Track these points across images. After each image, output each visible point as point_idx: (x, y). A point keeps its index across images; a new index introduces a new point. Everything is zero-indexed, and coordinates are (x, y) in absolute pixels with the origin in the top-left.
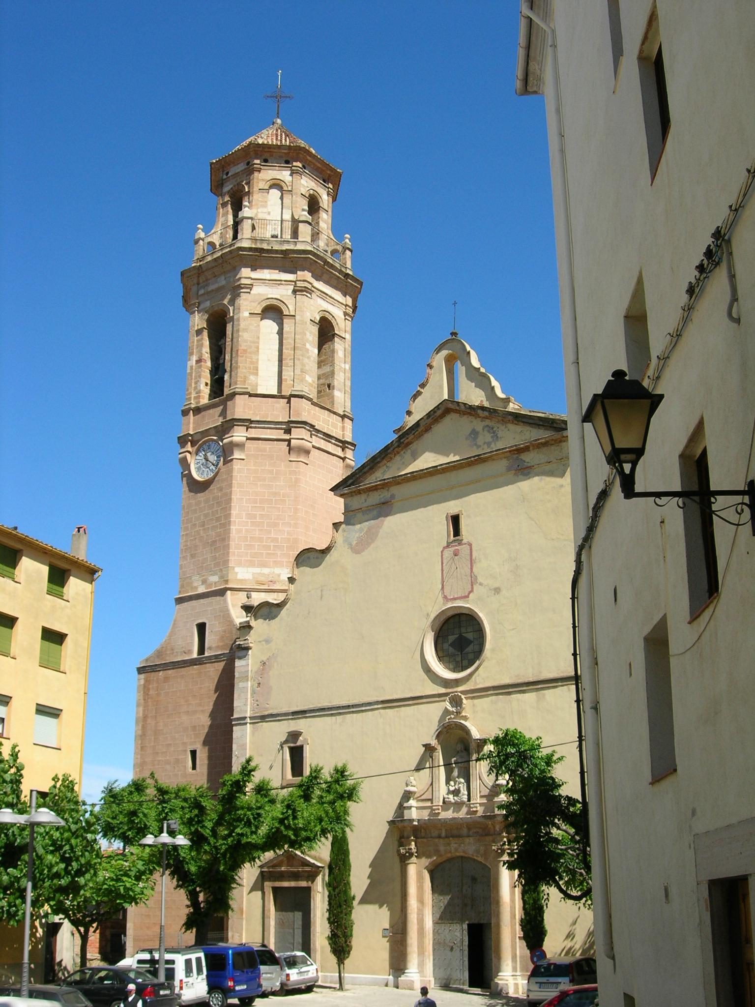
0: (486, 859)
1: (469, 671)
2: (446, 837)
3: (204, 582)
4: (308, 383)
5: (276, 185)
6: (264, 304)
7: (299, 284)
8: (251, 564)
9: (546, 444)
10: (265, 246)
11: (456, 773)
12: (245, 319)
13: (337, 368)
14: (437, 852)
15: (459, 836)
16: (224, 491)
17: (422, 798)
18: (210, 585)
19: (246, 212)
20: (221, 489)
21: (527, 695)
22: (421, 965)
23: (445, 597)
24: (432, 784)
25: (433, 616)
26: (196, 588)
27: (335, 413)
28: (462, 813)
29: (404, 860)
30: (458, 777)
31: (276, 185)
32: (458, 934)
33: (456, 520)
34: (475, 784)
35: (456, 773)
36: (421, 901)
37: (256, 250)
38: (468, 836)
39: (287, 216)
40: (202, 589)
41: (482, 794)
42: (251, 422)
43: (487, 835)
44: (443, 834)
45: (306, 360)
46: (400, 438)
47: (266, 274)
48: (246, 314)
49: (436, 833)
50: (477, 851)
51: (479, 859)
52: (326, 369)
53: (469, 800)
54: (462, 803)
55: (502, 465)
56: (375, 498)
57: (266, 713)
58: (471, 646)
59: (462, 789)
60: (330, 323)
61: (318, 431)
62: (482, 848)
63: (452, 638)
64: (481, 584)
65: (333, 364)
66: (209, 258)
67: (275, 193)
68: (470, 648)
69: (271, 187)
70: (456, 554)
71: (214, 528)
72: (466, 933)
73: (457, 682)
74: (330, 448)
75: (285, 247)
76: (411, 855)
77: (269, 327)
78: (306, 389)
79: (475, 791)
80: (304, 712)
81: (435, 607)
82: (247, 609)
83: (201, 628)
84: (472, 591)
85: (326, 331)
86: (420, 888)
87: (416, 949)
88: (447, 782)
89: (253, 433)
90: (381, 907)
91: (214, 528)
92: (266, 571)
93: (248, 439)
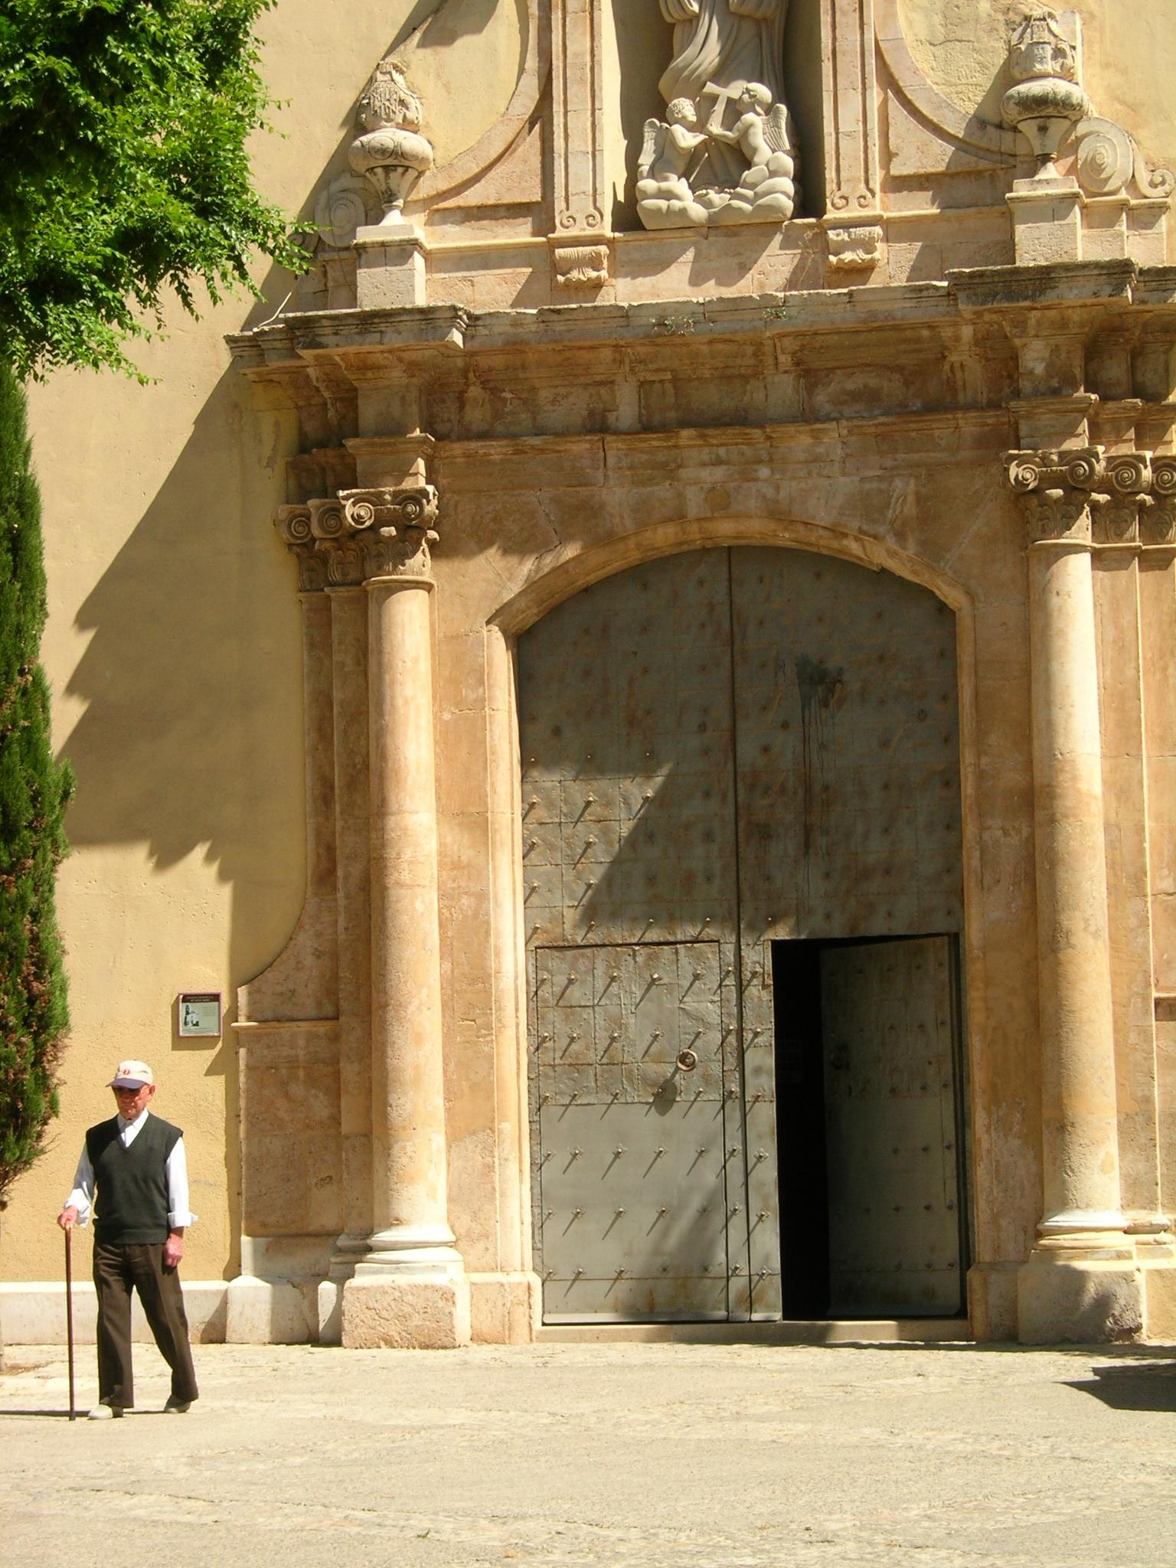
0: (932, 551)
2: (646, 427)
11: (705, 50)
14: (580, 516)
15: (741, 419)
17: (472, 197)
22: (471, 1198)
24: (541, 115)
28: (772, 271)
29: (341, 578)
30: (722, 74)
32: (708, 1006)
34: (847, 113)
35: (705, 50)
36: (468, 814)
38: (807, 416)
41: (897, 170)
43: (933, 407)
44: (626, 409)
49: (576, 404)
50: (871, 507)
51: (884, 554)
53: (810, 196)
54: (764, 226)
59: (759, 139)
62: (904, 488)
72: (761, 998)
76: (411, 532)
79: (851, 148)
86: (461, 738)
87: (438, 1102)
88: (645, 103)
90: (167, 856)
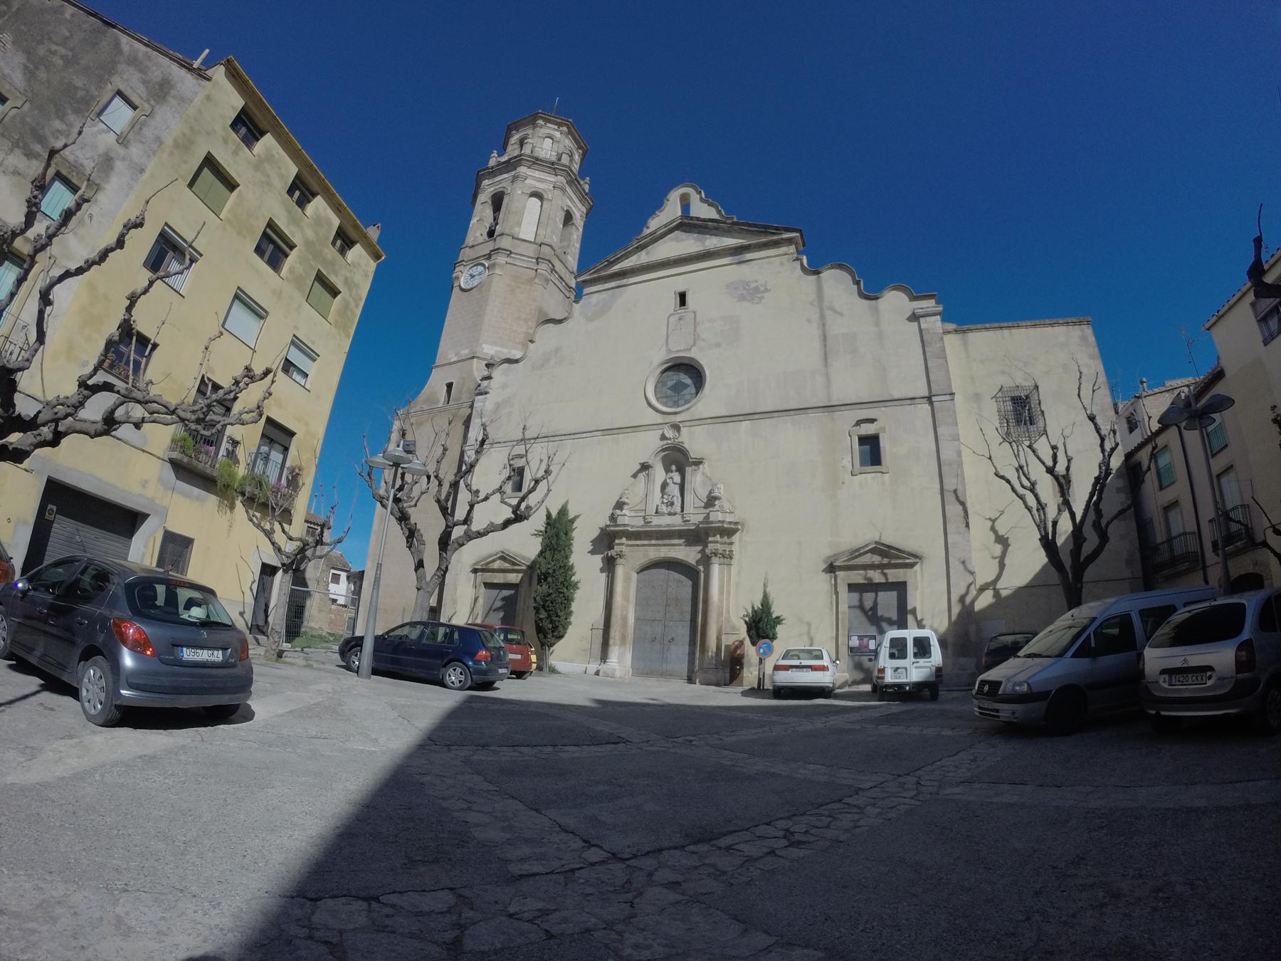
8: (494, 344)
23: (669, 351)
33: (682, 298)
47: (537, 174)
52: (565, 244)
63: (670, 383)
73: (675, 413)
81: (659, 357)
83: (450, 386)
85: (568, 218)
92: (505, 350)
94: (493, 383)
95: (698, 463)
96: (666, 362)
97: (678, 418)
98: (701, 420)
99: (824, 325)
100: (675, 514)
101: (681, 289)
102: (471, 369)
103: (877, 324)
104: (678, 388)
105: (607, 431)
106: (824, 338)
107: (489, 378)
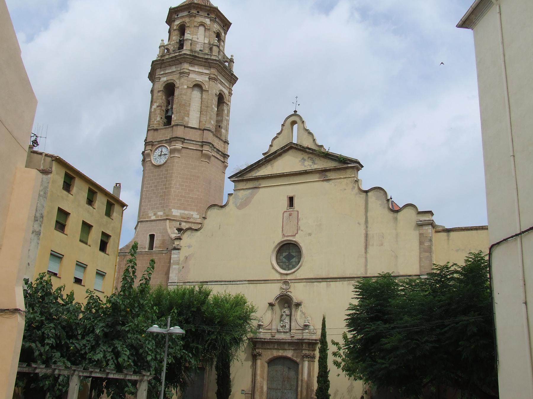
1: (293, 270)
3: (155, 214)
4: (211, 124)
5: (202, 24)
6: (194, 83)
7: (212, 76)
8: (179, 208)
9: (339, 169)
10: (196, 54)
12: (184, 89)
13: (224, 118)
16: (169, 172)
18: (158, 216)
19: (187, 36)
20: (167, 170)
21: (322, 283)
23: (284, 235)
25: (277, 242)
26: (150, 217)
27: (222, 140)
31: (202, 24)
33: (291, 200)
37: (193, 56)
39: (207, 42)
40: (153, 218)
42: (185, 139)
45: (212, 113)
46: (266, 158)
47: (196, 69)
48: (186, 87)
50: (293, 356)
52: (219, 118)
55: (316, 177)
56: (251, 185)
57: (186, 281)
58: (294, 259)
60: (222, 96)
61: (215, 148)
63: (285, 254)
64: (302, 231)
65: (222, 116)
66: (167, 57)
67: (202, 29)
68: (294, 260)
69: (200, 25)
70: (290, 215)
71: (162, 189)
73: (287, 274)
74: (219, 157)
75: (206, 57)
77: (196, 94)
78: (211, 127)
80: (207, 282)
81: (278, 239)
82: (179, 230)
83: (152, 237)
84: (297, 233)
89: (185, 145)
91: (162, 189)
92: (186, 212)
93: (182, 147)
94: (182, 243)
95: (298, 305)
96: (282, 242)
97: (289, 277)
98: (301, 280)
99: (367, 227)
100: (287, 332)
101: (291, 195)
102: (166, 225)
103: (396, 229)
104: (289, 258)
105: (251, 282)
106: (366, 236)
107: (179, 239)
